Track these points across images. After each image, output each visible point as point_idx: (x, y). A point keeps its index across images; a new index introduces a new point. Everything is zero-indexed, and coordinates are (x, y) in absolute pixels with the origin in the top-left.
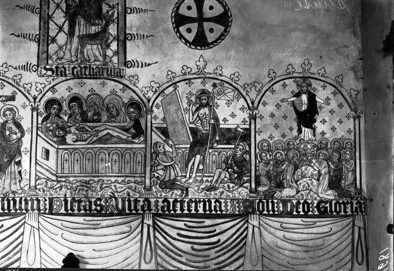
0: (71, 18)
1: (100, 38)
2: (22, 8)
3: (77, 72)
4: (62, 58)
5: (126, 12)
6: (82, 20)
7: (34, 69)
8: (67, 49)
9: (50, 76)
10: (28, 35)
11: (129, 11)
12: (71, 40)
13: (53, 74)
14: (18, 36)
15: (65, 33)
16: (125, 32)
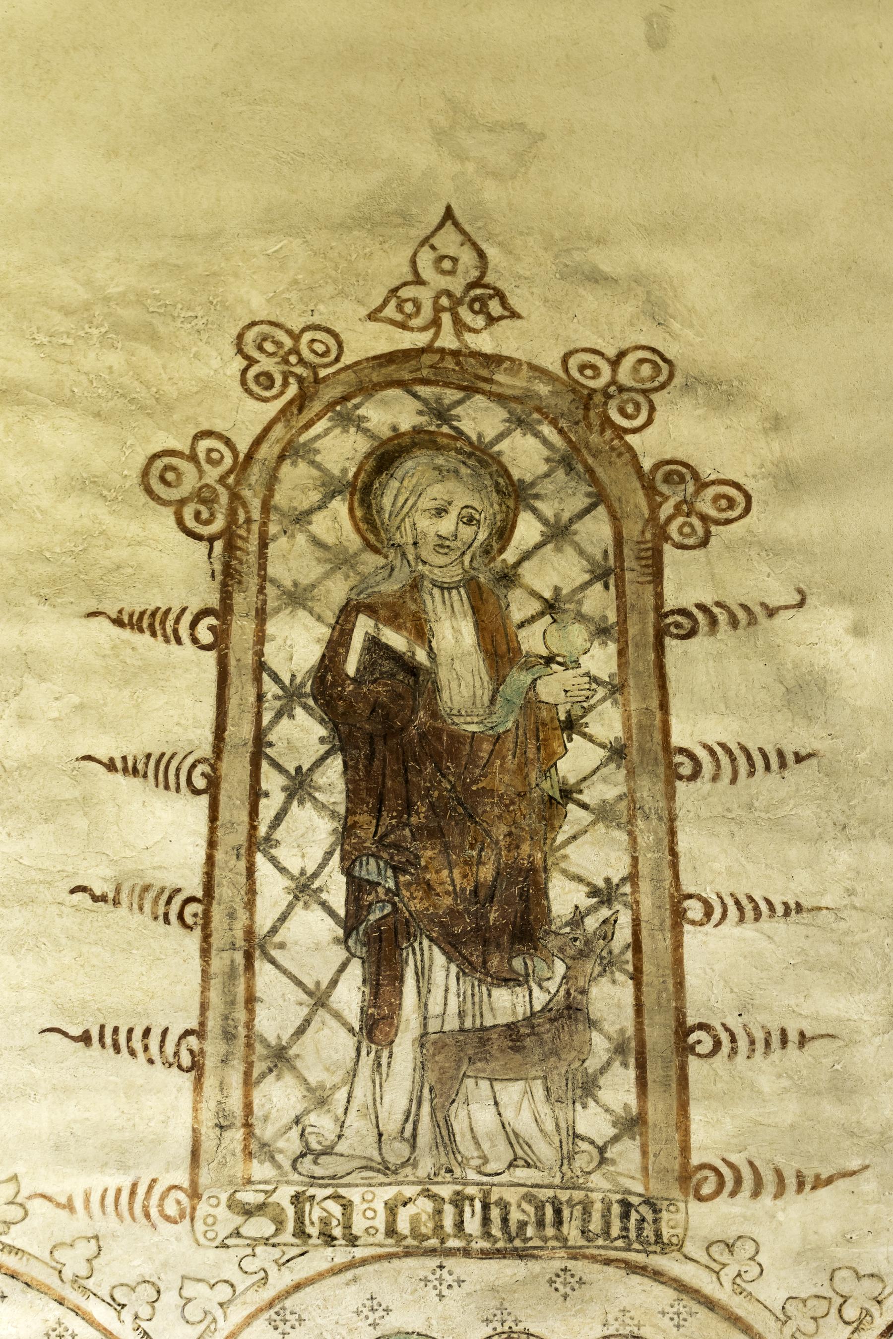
0: (380, 943)
1: (541, 1041)
2: (103, 898)
3: (415, 1221)
4: (328, 1151)
5: (679, 916)
6: (439, 958)
7: (171, 1210)
8: (355, 1105)
9: (266, 1241)
10: (137, 1034)
11: (695, 910)
12: (378, 1058)
13: (274, 1235)
14: (85, 1038)
15: (345, 1024)
16: (680, 1014)
